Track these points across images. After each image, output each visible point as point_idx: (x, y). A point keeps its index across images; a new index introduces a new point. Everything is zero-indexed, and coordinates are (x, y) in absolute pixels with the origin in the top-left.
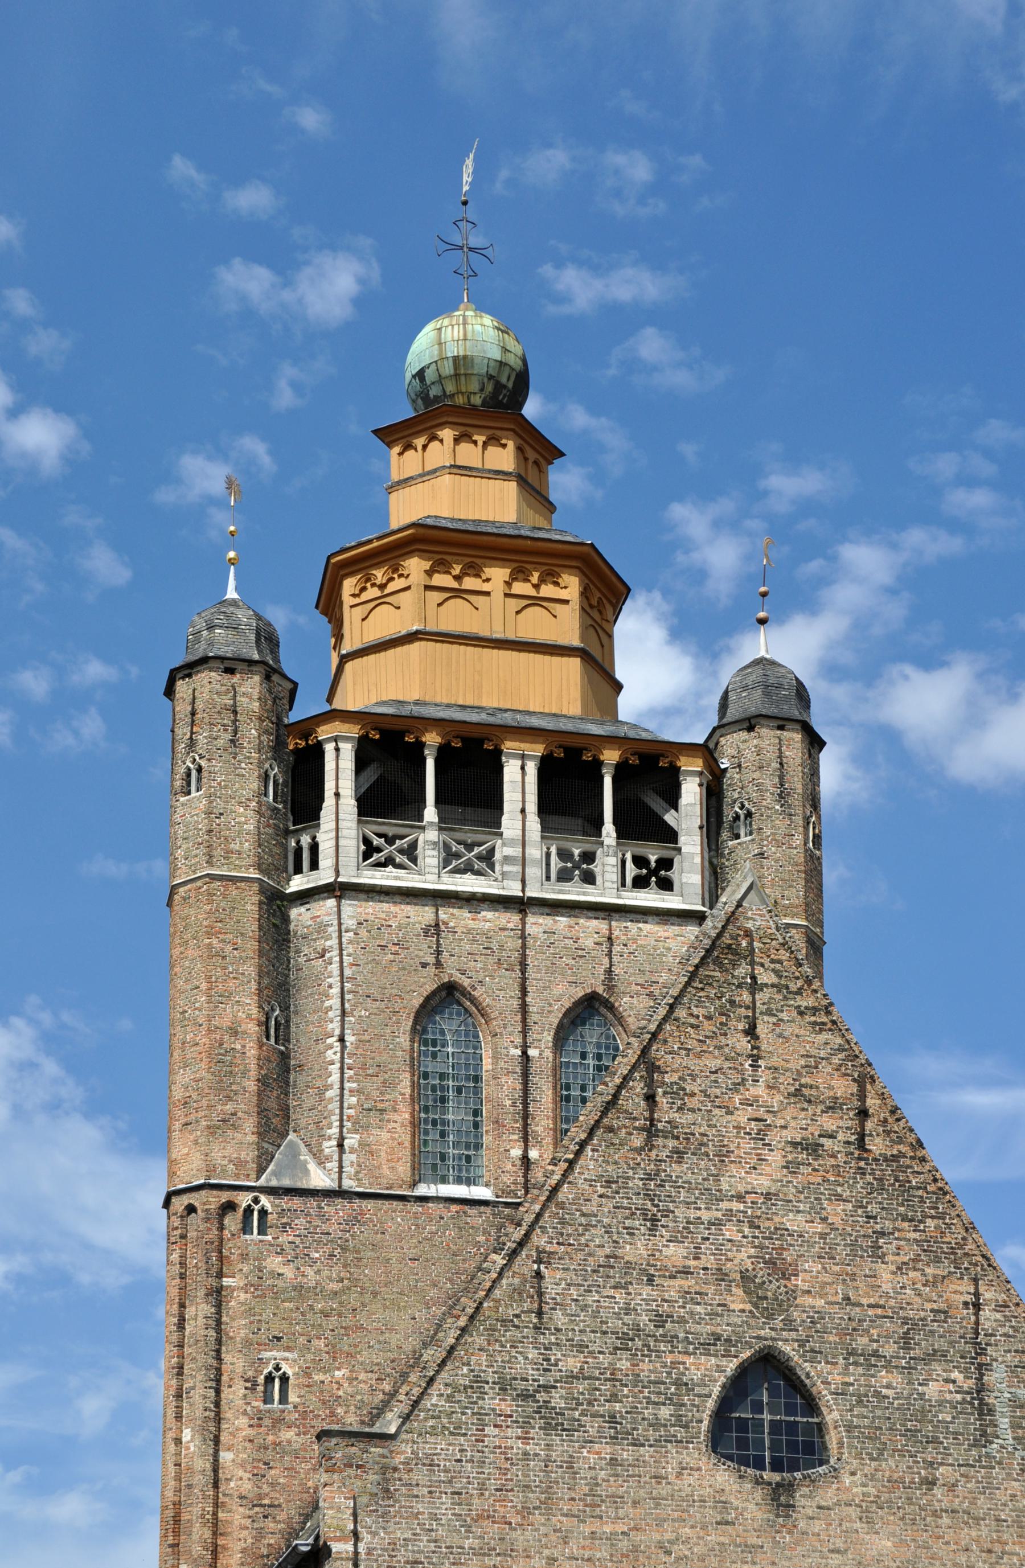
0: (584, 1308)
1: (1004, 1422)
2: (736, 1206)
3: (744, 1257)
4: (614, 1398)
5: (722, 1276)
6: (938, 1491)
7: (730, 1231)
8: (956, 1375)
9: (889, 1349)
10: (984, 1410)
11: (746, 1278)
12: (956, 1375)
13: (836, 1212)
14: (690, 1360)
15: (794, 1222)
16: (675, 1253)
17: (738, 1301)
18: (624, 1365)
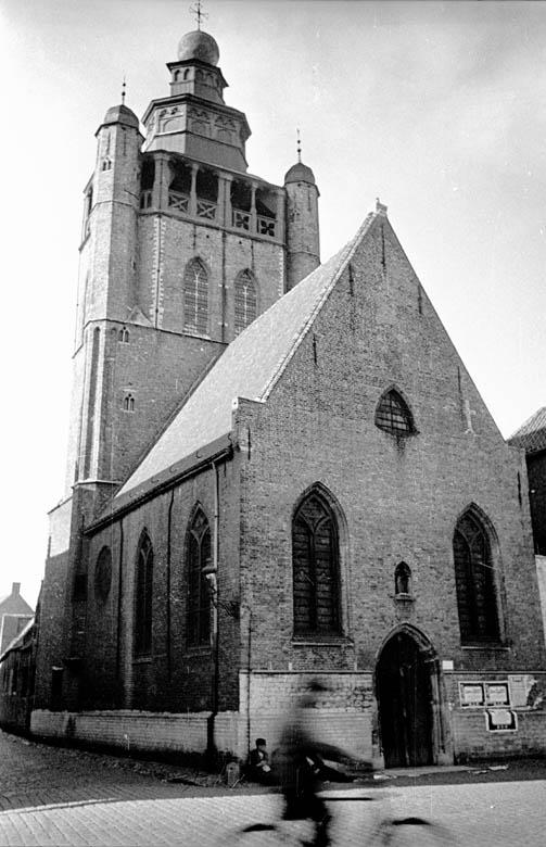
0: (331, 361)
1: (469, 423)
2: (381, 328)
3: (384, 349)
4: (342, 399)
5: (377, 354)
6: (450, 447)
7: (379, 338)
8: (455, 404)
9: (433, 391)
10: (463, 417)
11: (386, 358)
12: (455, 404)
13: (414, 335)
14: (368, 387)
15: (400, 337)
16: (361, 344)
17: (382, 365)
18: (346, 385)
